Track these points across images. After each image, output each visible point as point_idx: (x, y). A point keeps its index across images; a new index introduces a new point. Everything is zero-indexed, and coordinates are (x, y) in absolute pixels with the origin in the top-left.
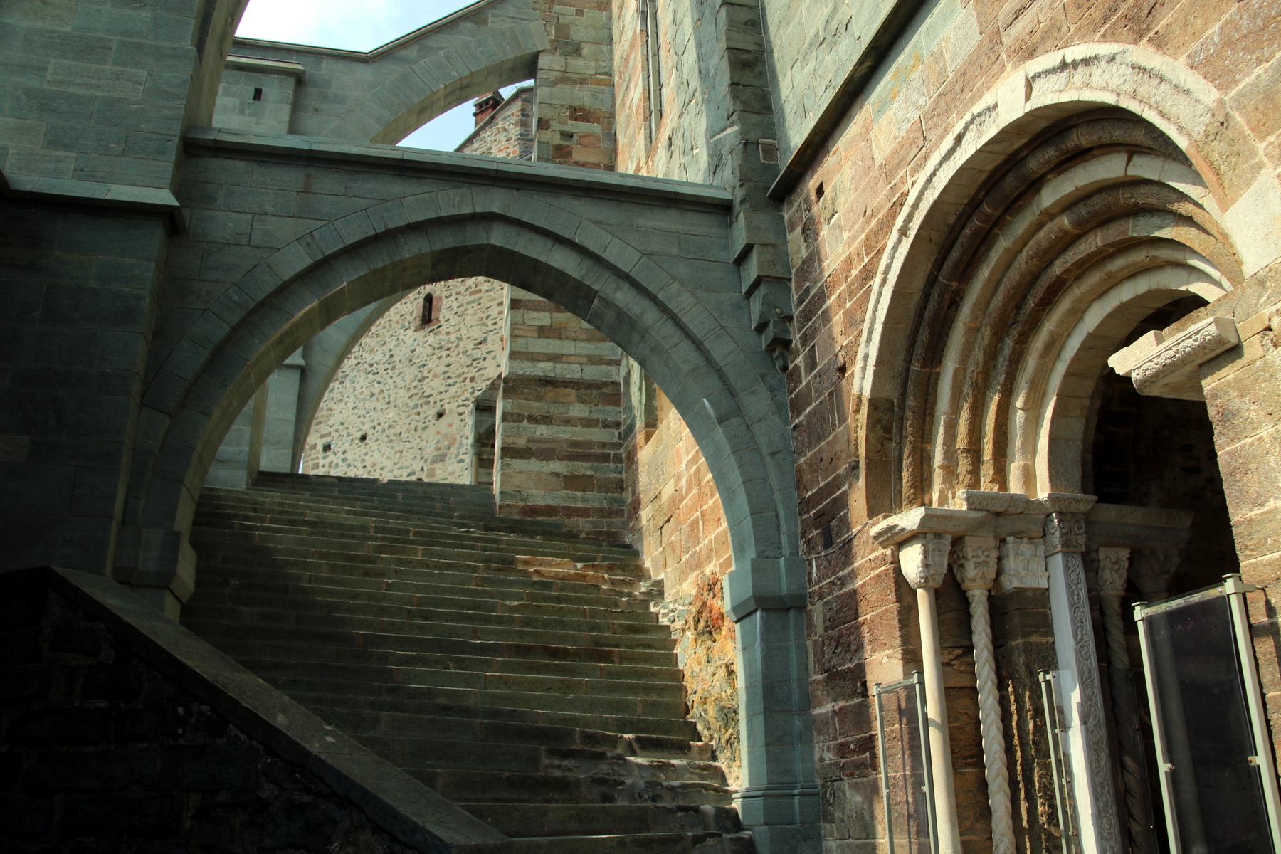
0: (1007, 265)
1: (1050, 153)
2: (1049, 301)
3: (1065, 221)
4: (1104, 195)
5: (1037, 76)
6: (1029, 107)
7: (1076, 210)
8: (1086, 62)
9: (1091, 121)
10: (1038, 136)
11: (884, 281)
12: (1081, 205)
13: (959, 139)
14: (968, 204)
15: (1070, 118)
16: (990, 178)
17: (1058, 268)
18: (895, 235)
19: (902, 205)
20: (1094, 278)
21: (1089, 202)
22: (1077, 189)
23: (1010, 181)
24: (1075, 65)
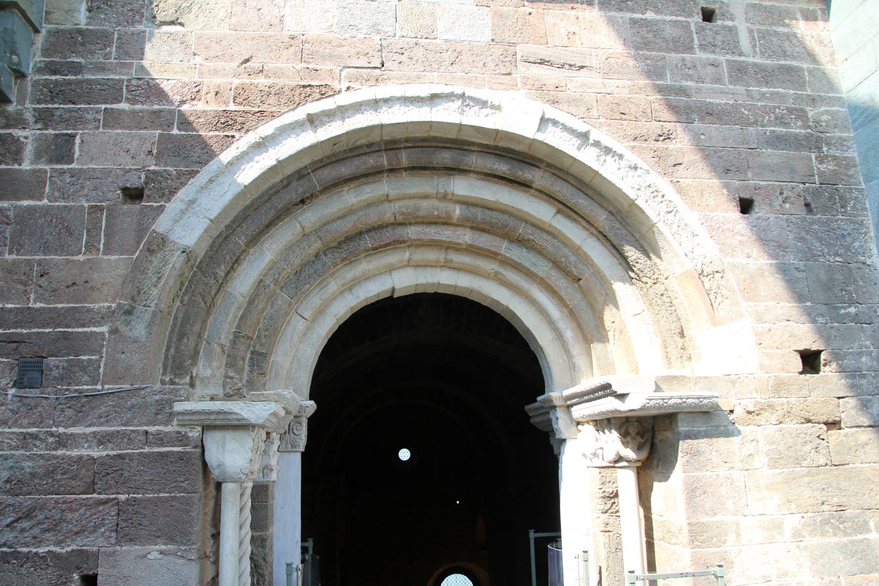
0: (369, 205)
1: (502, 167)
2: (377, 249)
3: (457, 211)
4: (506, 217)
5: (555, 123)
6: (540, 137)
7: (473, 210)
8: (608, 151)
9: (554, 174)
10: (496, 148)
11: (261, 145)
12: (479, 209)
13: (434, 98)
14: (387, 143)
15: (541, 161)
16: (424, 140)
17: (412, 232)
18: (301, 113)
19: (323, 96)
20: (432, 255)
21: (490, 212)
22: (496, 203)
23: (445, 157)
24: (597, 144)
